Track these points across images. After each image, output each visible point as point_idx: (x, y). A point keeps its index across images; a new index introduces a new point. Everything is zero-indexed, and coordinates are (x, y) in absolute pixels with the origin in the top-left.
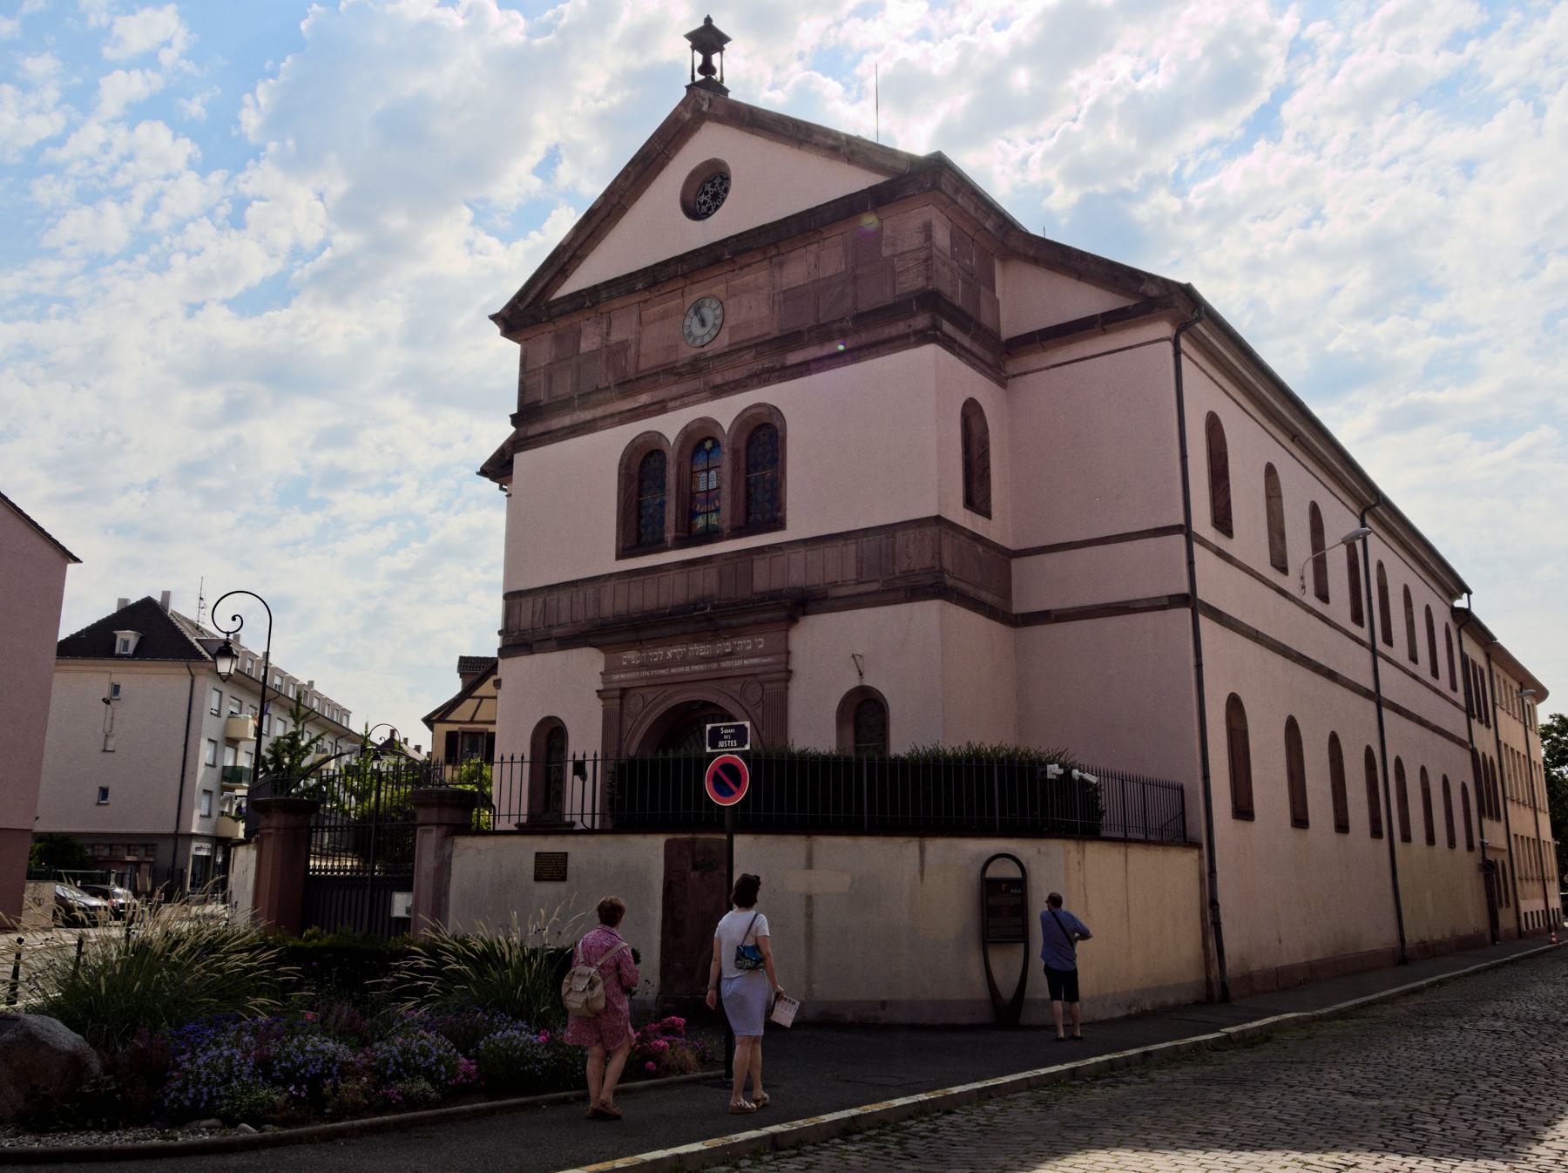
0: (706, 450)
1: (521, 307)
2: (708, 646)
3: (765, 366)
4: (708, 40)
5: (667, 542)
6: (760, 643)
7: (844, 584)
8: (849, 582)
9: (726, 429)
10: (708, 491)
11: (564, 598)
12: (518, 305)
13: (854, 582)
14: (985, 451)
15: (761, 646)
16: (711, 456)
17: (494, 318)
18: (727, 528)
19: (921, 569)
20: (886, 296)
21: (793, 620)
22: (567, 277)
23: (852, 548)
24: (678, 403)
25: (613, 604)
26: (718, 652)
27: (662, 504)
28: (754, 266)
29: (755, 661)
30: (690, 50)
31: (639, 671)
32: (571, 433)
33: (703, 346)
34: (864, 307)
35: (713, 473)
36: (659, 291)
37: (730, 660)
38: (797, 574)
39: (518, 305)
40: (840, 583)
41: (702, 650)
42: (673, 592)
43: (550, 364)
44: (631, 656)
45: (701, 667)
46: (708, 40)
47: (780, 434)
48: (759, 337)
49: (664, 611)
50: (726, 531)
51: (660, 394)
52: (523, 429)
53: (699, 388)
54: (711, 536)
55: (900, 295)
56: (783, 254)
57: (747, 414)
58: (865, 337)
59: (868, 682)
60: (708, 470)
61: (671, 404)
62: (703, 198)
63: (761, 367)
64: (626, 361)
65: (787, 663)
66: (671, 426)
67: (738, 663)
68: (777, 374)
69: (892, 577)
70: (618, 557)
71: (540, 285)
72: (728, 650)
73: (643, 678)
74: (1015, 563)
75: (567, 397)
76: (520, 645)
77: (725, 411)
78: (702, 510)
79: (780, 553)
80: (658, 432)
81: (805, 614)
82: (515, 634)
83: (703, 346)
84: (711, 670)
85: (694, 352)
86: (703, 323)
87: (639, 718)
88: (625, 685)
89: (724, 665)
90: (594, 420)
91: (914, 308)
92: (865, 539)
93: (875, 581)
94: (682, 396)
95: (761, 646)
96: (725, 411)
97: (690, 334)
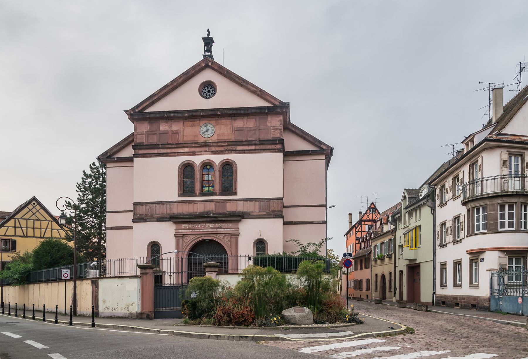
1: (137, 110)
4: (208, 42)
5: (197, 194)
6: (230, 225)
11: (158, 206)
12: (136, 109)
15: (230, 226)
20: (269, 137)
21: (240, 221)
23: (257, 203)
24: (199, 153)
25: (177, 210)
27: (193, 183)
33: (207, 138)
34: (262, 138)
37: (221, 229)
38: (241, 207)
39: (136, 109)
40: (254, 211)
42: (199, 208)
44: (186, 226)
45: (211, 230)
46: (208, 42)
48: (227, 139)
51: (192, 150)
52: (137, 151)
58: (262, 147)
59: (262, 237)
61: (196, 153)
66: (198, 160)
75: (156, 144)
77: (217, 159)
81: (244, 218)
87: (188, 243)
89: (218, 230)
90: (168, 153)
96: (217, 159)
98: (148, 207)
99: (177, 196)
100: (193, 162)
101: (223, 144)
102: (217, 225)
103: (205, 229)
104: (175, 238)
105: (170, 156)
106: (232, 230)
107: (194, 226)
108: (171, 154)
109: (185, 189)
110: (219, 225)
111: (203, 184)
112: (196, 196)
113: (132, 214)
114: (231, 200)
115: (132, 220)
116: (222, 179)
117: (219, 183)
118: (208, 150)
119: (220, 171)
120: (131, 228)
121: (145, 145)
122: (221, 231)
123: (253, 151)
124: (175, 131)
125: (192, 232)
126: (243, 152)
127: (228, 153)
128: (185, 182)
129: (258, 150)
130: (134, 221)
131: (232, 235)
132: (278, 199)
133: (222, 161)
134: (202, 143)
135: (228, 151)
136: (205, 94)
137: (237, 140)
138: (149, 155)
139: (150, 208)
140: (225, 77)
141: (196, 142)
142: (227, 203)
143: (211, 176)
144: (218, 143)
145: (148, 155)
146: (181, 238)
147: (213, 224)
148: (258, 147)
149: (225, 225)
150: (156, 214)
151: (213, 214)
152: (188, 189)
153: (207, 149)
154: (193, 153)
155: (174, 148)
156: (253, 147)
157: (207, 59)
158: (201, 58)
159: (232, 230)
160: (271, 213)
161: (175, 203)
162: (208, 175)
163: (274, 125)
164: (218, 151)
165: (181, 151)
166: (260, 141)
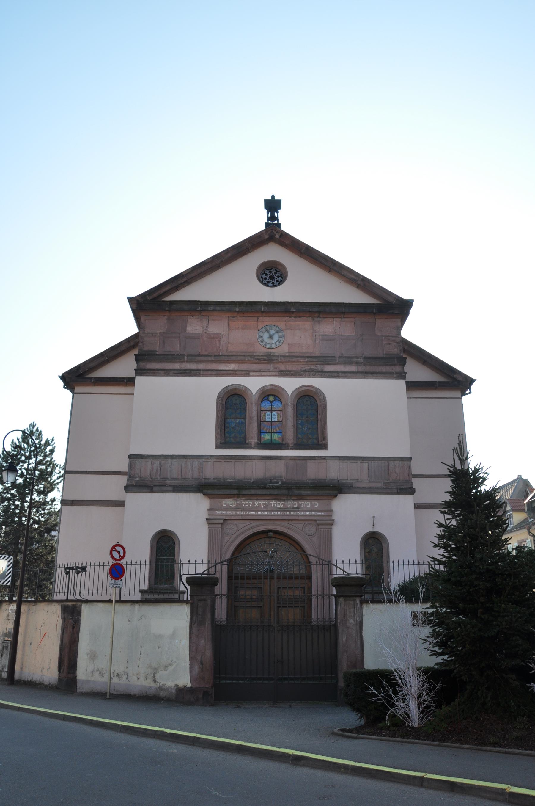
1: (149, 298)
3: (312, 368)
6: (316, 504)
7: (362, 481)
11: (176, 464)
16: (273, 404)
18: (292, 444)
19: (403, 480)
23: (365, 465)
24: (257, 373)
26: (289, 506)
27: (243, 425)
28: (302, 318)
29: (313, 513)
31: (236, 511)
32: (181, 373)
35: (274, 413)
36: (243, 314)
37: (298, 511)
41: (278, 504)
43: (163, 333)
44: (230, 502)
45: (279, 513)
51: (244, 367)
52: (142, 364)
53: (270, 370)
56: (320, 317)
57: (303, 389)
58: (368, 368)
59: (377, 529)
60: (271, 411)
61: (251, 373)
62: (264, 276)
63: (309, 368)
64: (220, 344)
65: (331, 516)
67: (303, 513)
68: (320, 373)
69: (388, 481)
70: (217, 447)
71: (164, 290)
72: (296, 506)
73: (238, 515)
75: (178, 353)
76: (140, 486)
78: (268, 431)
79: (324, 461)
81: (341, 493)
84: (285, 515)
85: (266, 350)
87: (234, 536)
88: (224, 517)
89: (293, 513)
90: (199, 370)
91: (396, 362)
92: (373, 462)
93: (379, 482)
94: (260, 371)
95: (316, 506)
97: (263, 341)
98: (157, 463)
99: (214, 447)
100: (246, 388)
102: (290, 504)
103: (267, 511)
105: (203, 375)
106: (319, 514)
107: (247, 504)
108: (205, 373)
110: (295, 504)
111: (262, 428)
112: (251, 448)
113: (126, 477)
114: (317, 458)
115: (125, 486)
118: (272, 369)
119: (294, 405)
120: (121, 503)
121: (159, 355)
123: (354, 375)
124: (213, 334)
125: (241, 515)
126: (336, 374)
127: (309, 376)
130: (128, 488)
131: (318, 525)
132: (402, 459)
133: (297, 389)
134: (262, 356)
135: (308, 372)
138: (165, 371)
139: (161, 467)
140: (300, 257)
141: (252, 354)
142: (308, 464)
144: (291, 357)
145: (163, 372)
146: (220, 526)
147: (284, 501)
149: (305, 504)
151: (283, 483)
153: (271, 367)
154: (245, 372)
155: (211, 362)
156: (353, 368)
157: (272, 229)
158: (263, 228)
159: (319, 514)
160: (391, 484)
161: (210, 460)
162: (271, 411)
163: (388, 335)
164: (290, 371)
165: (223, 369)
166: (365, 358)
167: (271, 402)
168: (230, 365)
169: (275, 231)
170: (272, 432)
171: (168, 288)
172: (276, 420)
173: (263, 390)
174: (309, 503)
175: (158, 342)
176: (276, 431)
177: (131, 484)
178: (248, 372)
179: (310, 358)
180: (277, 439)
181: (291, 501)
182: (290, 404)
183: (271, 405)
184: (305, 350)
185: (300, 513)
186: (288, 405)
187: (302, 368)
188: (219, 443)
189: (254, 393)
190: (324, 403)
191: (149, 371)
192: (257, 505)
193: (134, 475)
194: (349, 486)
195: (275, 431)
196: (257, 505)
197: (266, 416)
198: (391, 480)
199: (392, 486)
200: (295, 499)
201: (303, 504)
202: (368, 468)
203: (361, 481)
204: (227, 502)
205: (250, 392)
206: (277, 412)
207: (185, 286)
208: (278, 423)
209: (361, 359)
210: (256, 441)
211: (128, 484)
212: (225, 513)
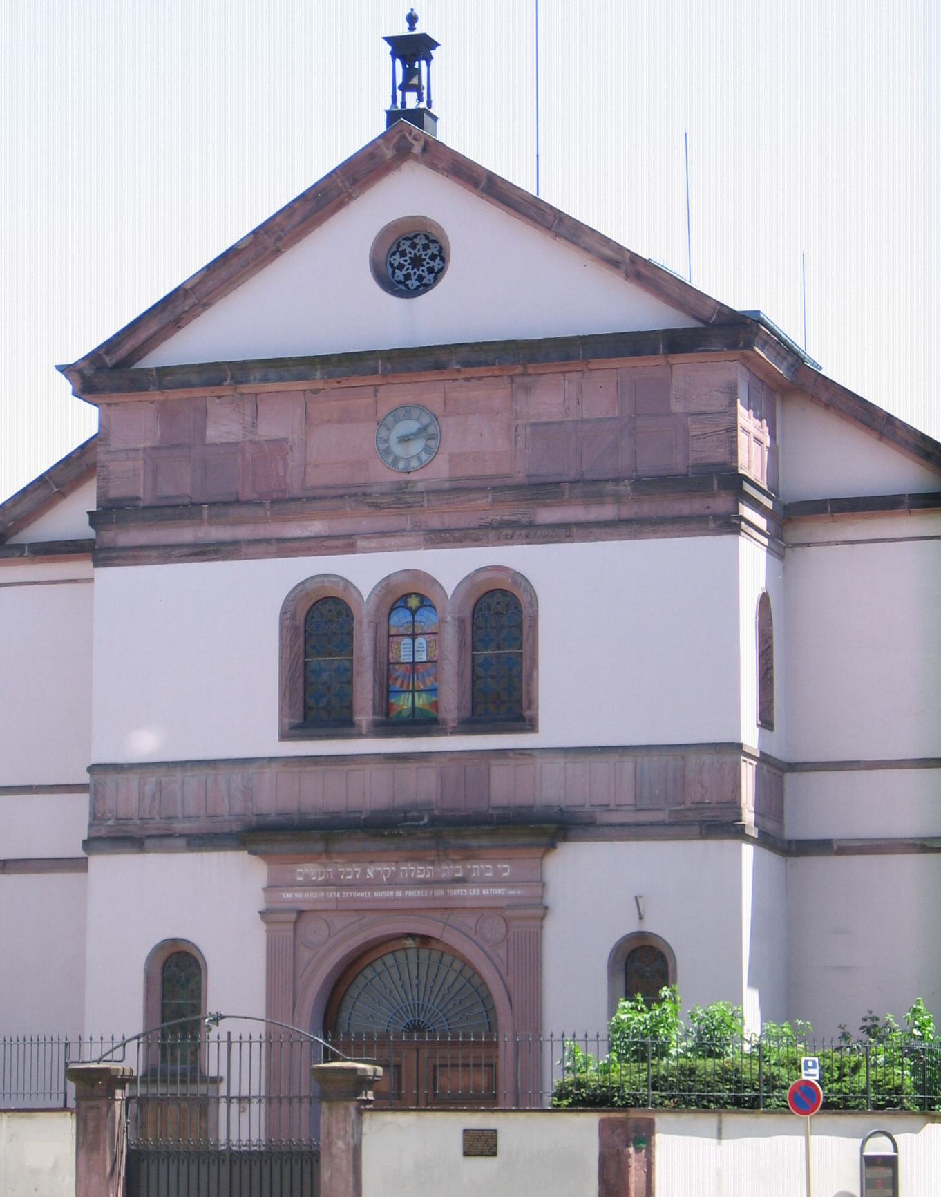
0: (410, 609)
1: (109, 361)
2: (429, 868)
5: (360, 726)
6: (505, 870)
7: (618, 809)
8: (624, 808)
9: (449, 593)
10: (414, 663)
11: (193, 781)
13: (629, 808)
14: (769, 647)
16: (417, 618)
17: (64, 369)
18: (453, 720)
19: (718, 803)
20: (678, 463)
21: (551, 846)
22: (180, 327)
23: (628, 765)
24: (373, 543)
26: (444, 875)
27: (346, 678)
28: (484, 379)
30: (389, 57)
31: (325, 891)
32: (196, 554)
35: (421, 641)
36: (339, 382)
40: (612, 807)
41: (422, 871)
43: (153, 448)
44: (310, 870)
45: (420, 893)
47: (526, 612)
48: (493, 477)
49: (357, 815)
50: (451, 724)
54: (424, 724)
55: (693, 466)
57: (482, 576)
58: (647, 508)
59: (650, 926)
60: (414, 636)
61: (361, 543)
62: (397, 260)
63: (498, 518)
64: (286, 469)
65: (542, 897)
67: (475, 892)
68: (523, 532)
69: (682, 807)
70: (284, 737)
72: (459, 875)
74: (789, 778)
75: (188, 501)
78: (405, 688)
80: (343, 579)
82: (111, 823)
83: (409, 473)
84: (434, 898)
85: (396, 477)
86: (405, 439)
89: (454, 893)
90: (235, 543)
97: (388, 451)
98: (151, 781)
101: (473, 500)
102: (448, 870)
104: (262, 927)
107: (348, 873)
109: (311, 703)
110: (458, 870)
112: (360, 736)
116: (473, 656)
117: (460, 675)
119: (461, 621)
122: (463, 898)
128: (313, 671)
129: (628, 522)
134: (383, 494)
136: (400, 275)
137: (535, 480)
141: (360, 490)
143: (425, 645)
145: (154, 553)
147: (432, 863)
148: (627, 512)
150: (187, 818)
152: (323, 702)
156: (608, 512)
167: (414, 612)
168: (309, 523)
169: (410, 134)
170: (416, 688)
171: (152, 328)
172: (424, 658)
173: (387, 585)
174: (490, 866)
175: (142, 473)
176: (425, 684)
177: (98, 834)
178: (351, 541)
179: (500, 488)
180: (427, 708)
181: (448, 865)
182: (449, 618)
183: (414, 622)
184: (490, 470)
185: (468, 892)
186: (446, 622)
187: (482, 519)
188: (287, 728)
189: (366, 594)
190: (531, 611)
191: (124, 554)
192: (372, 876)
193: (103, 815)
194: (587, 821)
195: (422, 687)
196: (372, 876)
197: (402, 650)
198: (688, 805)
199: (690, 818)
200: (456, 858)
201: (476, 869)
202: (635, 773)
203: (615, 808)
204: (306, 870)
205: (356, 594)
206: (427, 636)
207: (199, 315)
208: (430, 664)
209: (625, 485)
210: (371, 717)
211: (92, 835)
212: (301, 896)
